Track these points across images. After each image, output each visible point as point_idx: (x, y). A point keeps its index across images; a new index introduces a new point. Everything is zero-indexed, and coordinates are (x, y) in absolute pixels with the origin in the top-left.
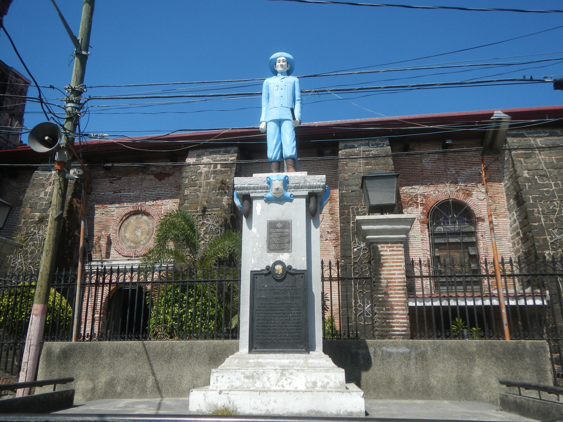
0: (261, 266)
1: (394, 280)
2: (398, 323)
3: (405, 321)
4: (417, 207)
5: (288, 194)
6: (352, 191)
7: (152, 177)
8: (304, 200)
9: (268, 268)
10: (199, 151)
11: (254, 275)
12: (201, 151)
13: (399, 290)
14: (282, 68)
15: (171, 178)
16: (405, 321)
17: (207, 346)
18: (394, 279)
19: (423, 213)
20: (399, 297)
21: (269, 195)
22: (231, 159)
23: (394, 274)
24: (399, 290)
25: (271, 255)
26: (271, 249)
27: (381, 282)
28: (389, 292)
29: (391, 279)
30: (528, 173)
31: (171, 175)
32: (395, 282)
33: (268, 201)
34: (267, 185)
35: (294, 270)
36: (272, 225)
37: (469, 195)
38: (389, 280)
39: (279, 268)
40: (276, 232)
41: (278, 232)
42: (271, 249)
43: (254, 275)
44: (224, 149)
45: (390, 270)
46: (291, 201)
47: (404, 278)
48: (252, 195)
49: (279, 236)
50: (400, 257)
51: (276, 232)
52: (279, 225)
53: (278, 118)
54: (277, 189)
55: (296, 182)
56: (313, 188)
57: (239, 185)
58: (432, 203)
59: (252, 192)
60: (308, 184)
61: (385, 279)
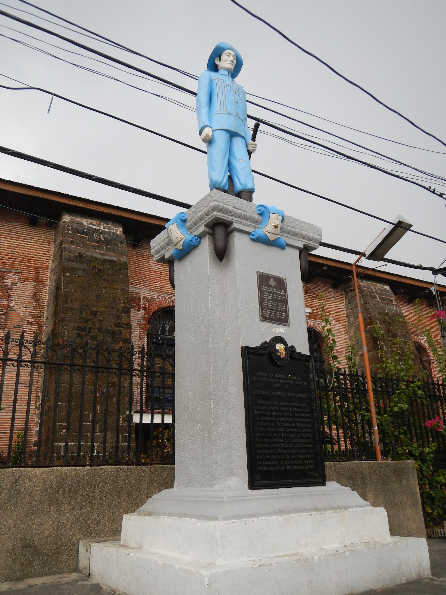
4: (139, 310)
6: (78, 276)
19: (143, 318)
25: (266, 325)
34: (257, 217)
35: (299, 353)
39: (279, 346)
40: (269, 292)
41: (271, 293)
51: (269, 292)
52: (272, 282)
53: (233, 130)
54: (276, 227)
55: (292, 225)
58: (154, 308)
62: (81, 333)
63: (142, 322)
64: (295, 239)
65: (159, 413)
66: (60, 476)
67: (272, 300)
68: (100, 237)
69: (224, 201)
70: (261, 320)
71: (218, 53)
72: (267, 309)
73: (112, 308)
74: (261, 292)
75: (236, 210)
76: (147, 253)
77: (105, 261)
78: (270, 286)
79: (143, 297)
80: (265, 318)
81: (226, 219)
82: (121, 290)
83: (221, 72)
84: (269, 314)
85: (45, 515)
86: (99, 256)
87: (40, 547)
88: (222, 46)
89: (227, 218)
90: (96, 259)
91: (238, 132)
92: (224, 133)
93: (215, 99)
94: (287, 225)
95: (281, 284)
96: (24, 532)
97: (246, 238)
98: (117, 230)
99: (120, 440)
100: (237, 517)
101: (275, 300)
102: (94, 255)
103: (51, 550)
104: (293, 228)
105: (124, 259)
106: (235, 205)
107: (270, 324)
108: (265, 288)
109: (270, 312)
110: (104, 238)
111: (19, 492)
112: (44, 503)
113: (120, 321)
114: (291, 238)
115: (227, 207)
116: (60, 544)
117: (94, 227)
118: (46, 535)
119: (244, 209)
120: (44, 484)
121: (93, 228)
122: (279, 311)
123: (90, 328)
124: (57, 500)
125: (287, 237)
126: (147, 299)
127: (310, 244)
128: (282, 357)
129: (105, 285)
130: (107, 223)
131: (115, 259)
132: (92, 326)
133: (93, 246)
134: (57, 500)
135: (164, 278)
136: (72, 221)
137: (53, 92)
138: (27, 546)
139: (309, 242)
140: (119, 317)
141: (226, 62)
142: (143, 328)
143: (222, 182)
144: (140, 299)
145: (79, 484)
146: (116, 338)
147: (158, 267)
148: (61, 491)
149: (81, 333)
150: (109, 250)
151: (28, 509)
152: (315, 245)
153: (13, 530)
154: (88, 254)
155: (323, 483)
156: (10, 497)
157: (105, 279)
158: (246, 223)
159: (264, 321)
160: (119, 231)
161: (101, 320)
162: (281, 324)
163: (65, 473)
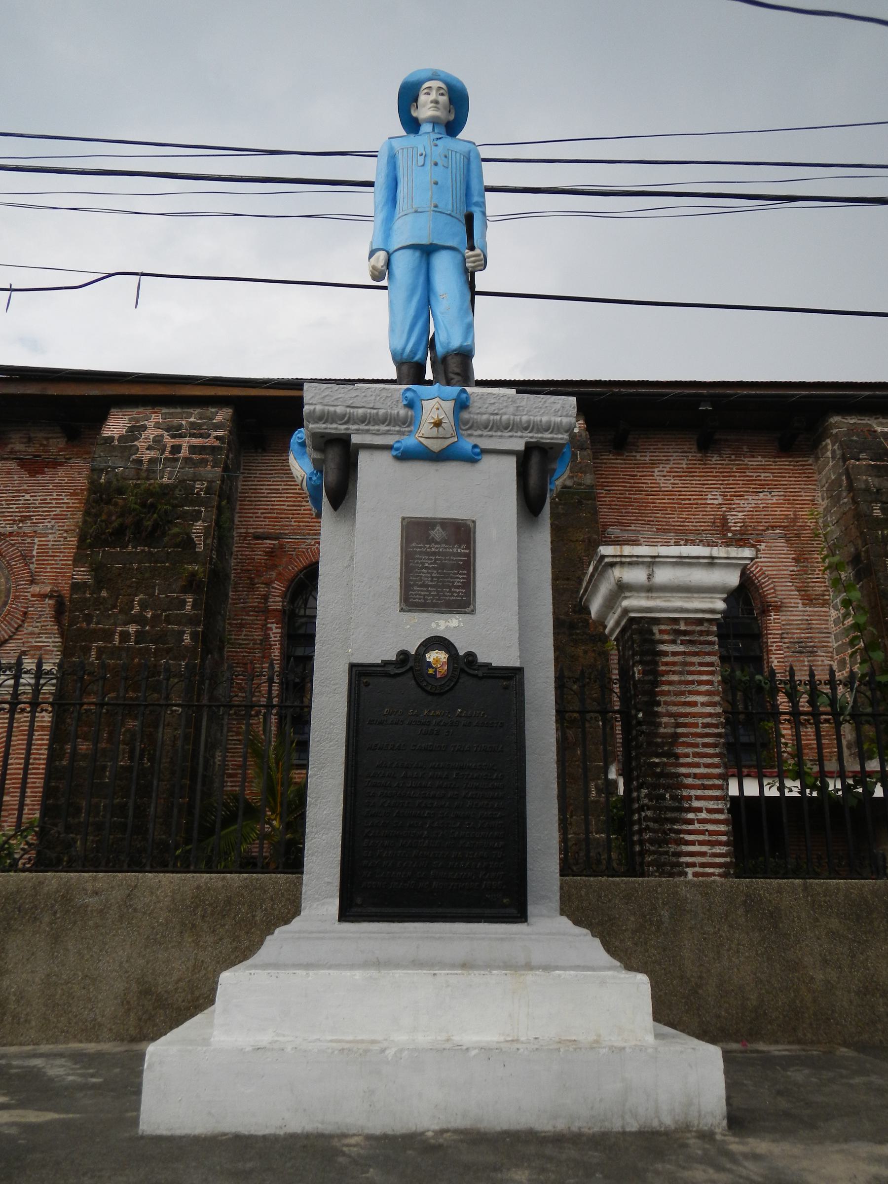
0: (380, 651)
1: (692, 720)
2: (702, 833)
3: (722, 828)
5: (467, 444)
7: (13, 465)
8: (511, 463)
9: (404, 656)
10: (136, 410)
11: (361, 675)
12: (141, 410)
13: (705, 745)
14: (438, 109)
15: (61, 472)
16: (722, 828)
17: (173, 891)
18: (694, 715)
20: (707, 766)
21: (409, 441)
22: (215, 434)
23: (694, 704)
24: (705, 745)
26: (412, 599)
27: (659, 725)
28: (680, 750)
29: (686, 715)
30: (881, 509)
31: (61, 464)
32: (696, 725)
33: (405, 456)
34: (402, 412)
35: (488, 666)
36: (416, 531)
38: (681, 720)
39: (437, 657)
40: (427, 553)
41: (434, 554)
42: (412, 599)
43: (361, 675)
44: (198, 411)
45: (682, 693)
47: (717, 715)
48: (355, 439)
49: (438, 564)
50: (708, 659)
51: (427, 553)
53: (425, 241)
54: (438, 424)
55: (492, 409)
56: (538, 431)
57: (319, 408)
59: (358, 431)
60: (525, 418)
61: (671, 715)
64: (501, 437)
65: (733, 776)
66: (198, 887)
67: (435, 568)
69: (326, 401)
70: (402, 610)
71: (408, 96)
72: (421, 586)
73: (568, 579)
75: (352, 410)
78: (433, 541)
81: (333, 431)
82: (583, 541)
83: (426, 128)
84: (424, 595)
85: (173, 947)
87: (166, 996)
88: (414, 79)
89: (336, 429)
91: (435, 242)
92: (408, 252)
94: (478, 414)
95: (462, 533)
96: (142, 970)
97: (385, 459)
99: (593, 828)
101: (443, 566)
103: (183, 1001)
104: (497, 414)
106: (349, 403)
107: (425, 615)
109: (427, 591)
111: (135, 910)
112: (174, 928)
114: (491, 436)
115: (332, 409)
116: (197, 993)
118: (175, 978)
119: (371, 405)
120: (173, 899)
122: (450, 587)
124: (194, 925)
125: (481, 436)
127: (542, 438)
128: (438, 676)
134: (194, 925)
135: (687, 502)
137: (139, 271)
139: (540, 435)
141: (427, 108)
143: (404, 349)
145: (228, 901)
146: (578, 634)
147: (672, 481)
148: (199, 912)
151: (148, 937)
152: (557, 439)
153: (126, 965)
155: (520, 915)
156: (121, 917)
158: (378, 430)
159: (409, 611)
162: (451, 612)
163: (206, 883)
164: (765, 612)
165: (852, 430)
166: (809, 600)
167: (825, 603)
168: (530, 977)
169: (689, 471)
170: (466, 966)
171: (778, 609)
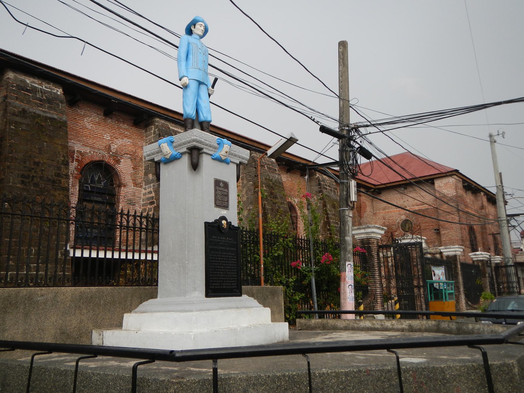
0: (211, 220)
6: (22, 130)
8: (235, 166)
19: (76, 169)
25: (217, 209)
34: (216, 145)
37: (118, 162)
39: (224, 222)
46: (228, 164)
52: (221, 184)
53: (201, 80)
54: (227, 152)
62: (25, 180)
63: (75, 172)
65: (79, 248)
66: (81, 292)
68: (42, 96)
71: (194, 23)
73: (53, 161)
74: (216, 190)
76: (83, 113)
77: (46, 118)
78: (220, 187)
79: (77, 151)
80: (217, 205)
82: (61, 145)
83: (194, 35)
86: (42, 113)
88: (197, 19)
90: (39, 116)
92: (196, 82)
93: (190, 56)
95: (226, 185)
97: (209, 157)
98: (58, 91)
99: (58, 270)
100: (201, 310)
101: (223, 195)
102: (37, 112)
105: (64, 118)
108: (218, 188)
110: (46, 97)
111: (58, 302)
113: (59, 172)
117: (37, 85)
118: (73, 327)
121: (36, 87)
123: (33, 177)
124: (80, 306)
126: (80, 152)
129: (46, 140)
130: (49, 84)
131: (55, 117)
132: (34, 175)
133: (36, 103)
136: (15, 77)
137: (86, 41)
138: (63, 333)
140: (59, 169)
141: (198, 30)
142: (76, 178)
144: (74, 152)
145: (91, 297)
146: (56, 186)
148: (82, 301)
149: (25, 180)
150: (50, 108)
153: (55, 323)
154: (31, 110)
155: (240, 295)
156: (52, 305)
157: (47, 134)
160: (59, 91)
161: (42, 170)
164: (120, 186)
165: (163, 125)
166: (136, 184)
167: (141, 187)
168: (252, 310)
169: (99, 123)
170: (237, 308)
171: (125, 186)
